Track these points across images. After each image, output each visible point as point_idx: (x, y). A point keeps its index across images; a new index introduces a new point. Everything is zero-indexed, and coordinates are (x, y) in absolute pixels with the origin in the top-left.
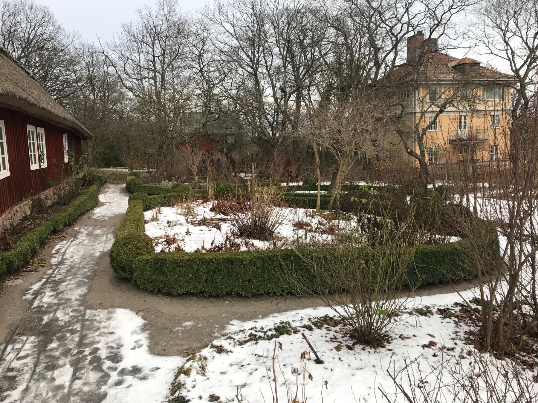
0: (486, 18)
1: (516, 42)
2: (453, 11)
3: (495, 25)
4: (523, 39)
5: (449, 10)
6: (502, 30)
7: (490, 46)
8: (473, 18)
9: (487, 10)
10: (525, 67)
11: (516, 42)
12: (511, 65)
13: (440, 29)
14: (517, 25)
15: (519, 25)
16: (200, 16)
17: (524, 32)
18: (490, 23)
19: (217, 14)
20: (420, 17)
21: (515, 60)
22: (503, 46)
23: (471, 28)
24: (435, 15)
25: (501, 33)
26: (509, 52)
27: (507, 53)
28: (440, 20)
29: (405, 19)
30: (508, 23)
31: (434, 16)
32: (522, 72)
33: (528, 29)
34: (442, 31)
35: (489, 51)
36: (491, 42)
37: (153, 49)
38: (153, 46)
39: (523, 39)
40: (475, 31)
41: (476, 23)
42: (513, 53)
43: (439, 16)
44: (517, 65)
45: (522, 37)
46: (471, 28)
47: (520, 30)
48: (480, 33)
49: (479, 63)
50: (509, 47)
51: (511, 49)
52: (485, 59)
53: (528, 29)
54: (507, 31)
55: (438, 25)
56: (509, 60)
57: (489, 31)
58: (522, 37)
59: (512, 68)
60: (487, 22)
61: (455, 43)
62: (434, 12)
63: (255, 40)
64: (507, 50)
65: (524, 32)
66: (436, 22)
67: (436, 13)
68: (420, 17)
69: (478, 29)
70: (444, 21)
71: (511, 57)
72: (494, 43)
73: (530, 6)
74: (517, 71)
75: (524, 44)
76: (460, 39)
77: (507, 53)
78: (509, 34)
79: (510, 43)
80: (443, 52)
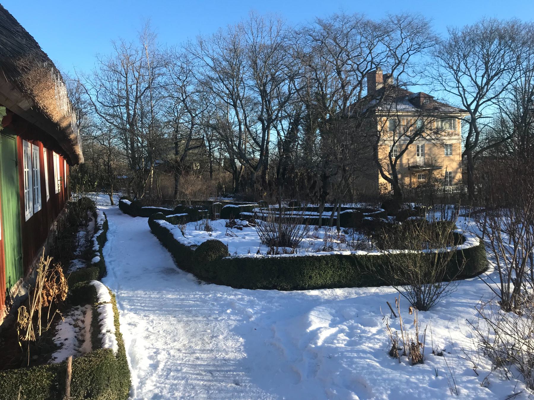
0: (440, 59)
1: (465, 81)
2: (411, 52)
3: (447, 66)
4: (472, 78)
5: (408, 52)
6: (454, 70)
7: (444, 83)
8: (428, 59)
9: (440, 52)
10: (475, 102)
11: (465, 81)
12: (463, 101)
13: (401, 68)
14: (466, 66)
15: (469, 65)
16: (184, 50)
17: (473, 72)
18: (443, 64)
19: (199, 49)
20: (383, 56)
21: (466, 95)
22: (454, 84)
23: (427, 68)
24: (396, 55)
25: (453, 72)
26: (461, 89)
27: (459, 90)
28: (400, 59)
29: (369, 58)
30: (459, 65)
31: (395, 55)
32: (473, 107)
33: (477, 70)
34: (402, 69)
35: (443, 88)
36: (444, 80)
37: (126, 78)
38: (126, 74)
39: (472, 78)
40: (430, 71)
41: (431, 63)
42: (464, 90)
43: (399, 56)
44: (468, 100)
45: (471, 76)
46: (427, 68)
47: (469, 71)
48: (435, 72)
49: (433, 97)
50: (460, 85)
51: (463, 87)
52: (438, 95)
53: (477, 70)
54: (459, 71)
55: (398, 64)
56: (461, 96)
57: (442, 70)
58: (471, 76)
59: (463, 103)
60: (440, 62)
61: (413, 80)
62: (395, 52)
63: (230, 74)
64: (458, 87)
65: (473, 72)
66: (397, 62)
67: (397, 53)
68: (383, 56)
69: (432, 69)
70: (404, 61)
71: (462, 93)
72: (447, 81)
73: (477, 49)
74: (468, 107)
75: (473, 83)
76: (418, 77)
77: (459, 90)
78: (460, 74)
79: (460, 80)
80: (403, 87)
